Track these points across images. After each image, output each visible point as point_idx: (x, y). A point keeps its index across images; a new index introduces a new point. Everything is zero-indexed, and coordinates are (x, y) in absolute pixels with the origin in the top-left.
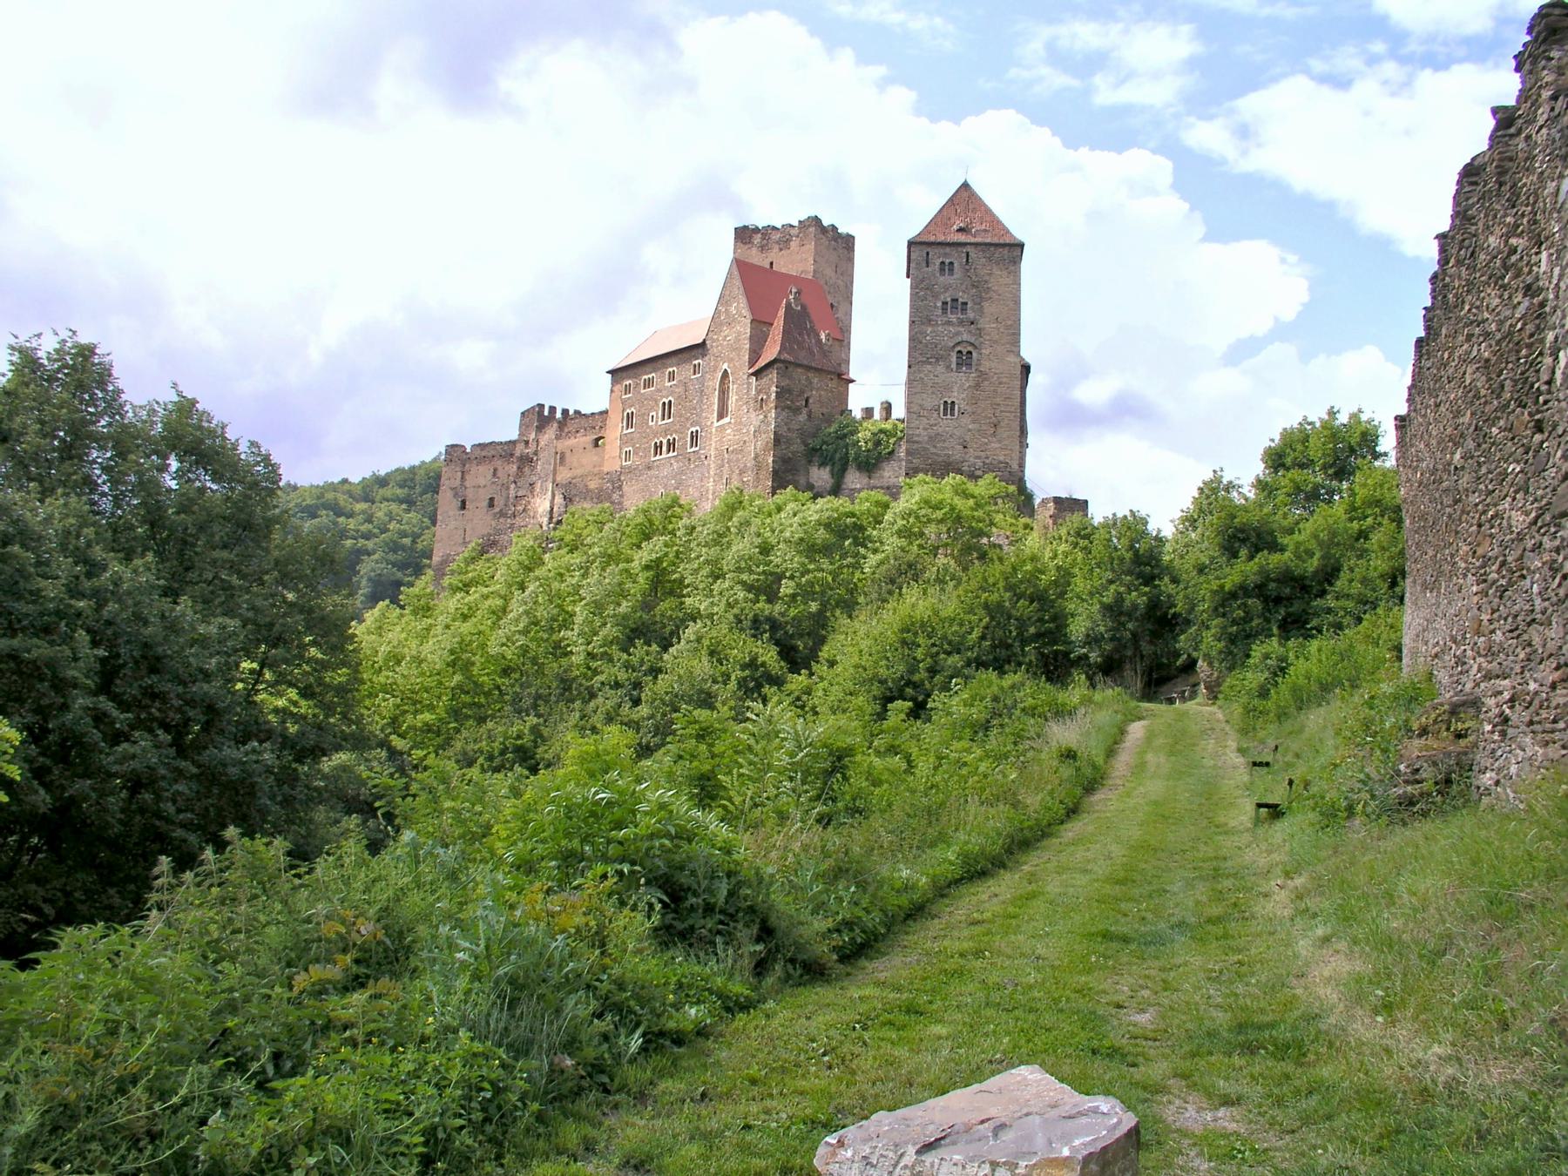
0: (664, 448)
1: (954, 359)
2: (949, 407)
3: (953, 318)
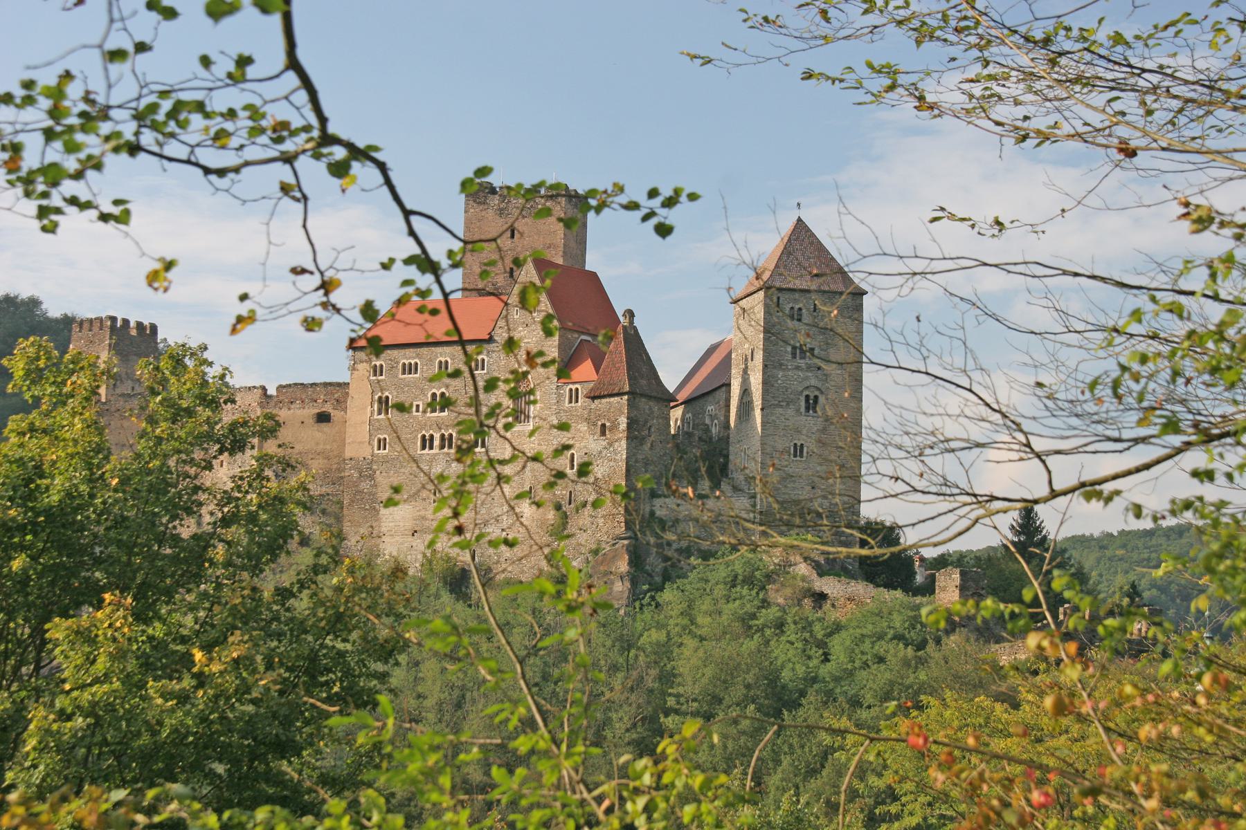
0: (437, 443)
1: (803, 404)
2: (798, 450)
3: (802, 363)
